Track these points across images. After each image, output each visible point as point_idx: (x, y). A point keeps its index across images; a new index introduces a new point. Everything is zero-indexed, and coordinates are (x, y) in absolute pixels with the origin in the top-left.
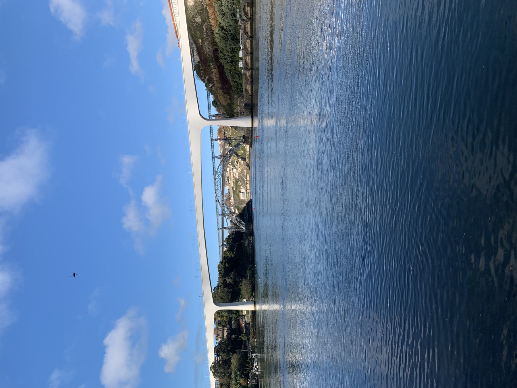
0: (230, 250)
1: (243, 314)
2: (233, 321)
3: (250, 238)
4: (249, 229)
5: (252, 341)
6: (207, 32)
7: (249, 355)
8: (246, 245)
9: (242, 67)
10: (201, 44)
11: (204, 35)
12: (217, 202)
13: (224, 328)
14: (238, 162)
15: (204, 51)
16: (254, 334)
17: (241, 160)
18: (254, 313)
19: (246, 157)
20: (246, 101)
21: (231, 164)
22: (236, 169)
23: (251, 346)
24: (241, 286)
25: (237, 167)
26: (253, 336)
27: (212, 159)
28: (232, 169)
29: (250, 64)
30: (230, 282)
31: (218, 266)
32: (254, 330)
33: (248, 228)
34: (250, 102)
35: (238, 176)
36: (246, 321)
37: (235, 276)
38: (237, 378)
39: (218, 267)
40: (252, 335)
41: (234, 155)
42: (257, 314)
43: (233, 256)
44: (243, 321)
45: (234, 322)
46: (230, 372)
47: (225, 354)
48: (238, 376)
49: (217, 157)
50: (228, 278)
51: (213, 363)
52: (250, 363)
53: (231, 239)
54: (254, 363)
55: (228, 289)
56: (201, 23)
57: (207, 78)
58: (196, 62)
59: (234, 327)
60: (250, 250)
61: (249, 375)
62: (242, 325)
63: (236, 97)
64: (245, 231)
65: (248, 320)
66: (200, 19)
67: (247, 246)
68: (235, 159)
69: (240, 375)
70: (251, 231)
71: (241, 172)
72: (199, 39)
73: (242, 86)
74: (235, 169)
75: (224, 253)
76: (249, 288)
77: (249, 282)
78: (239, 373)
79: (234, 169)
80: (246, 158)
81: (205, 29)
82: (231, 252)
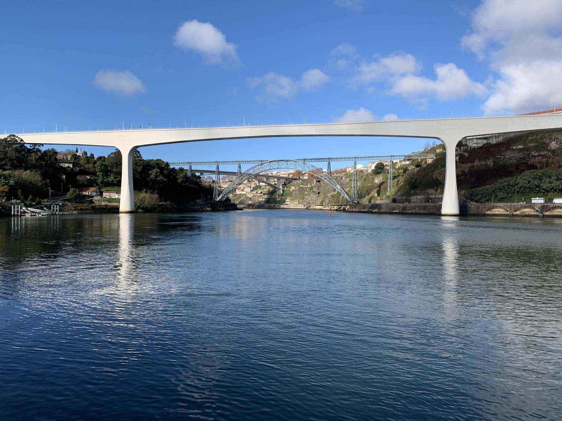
0: (186, 179)
1: (104, 194)
2: (89, 177)
3: (208, 207)
4: (218, 205)
5: (70, 206)
6: (539, 156)
7: (46, 200)
8: (198, 201)
9: (532, 202)
10: (515, 148)
11: (533, 152)
12: (260, 162)
13: (71, 163)
14: (262, 194)
15: (506, 151)
16: (81, 209)
17: (266, 197)
18: (115, 210)
19: (272, 205)
20: (472, 206)
21: (257, 186)
22: (250, 191)
23: (61, 204)
24: (146, 192)
25: (255, 192)
26: (78, 208)
27: (327, 157)
28: (250, 187)
29: (552, 214)
30: (151, 174)
31: (161, 160)
32: (88, 209)
33: (219, 205)
34: (472, 212)
35: (241, 194)
36: (92, 197)
37: (160, 182)
38: (2, 178)
39: (158, 160)
40: (79, 206)
41: (271, 189)
42: (116, 215)
43: (179, 181)
44: (93, 193)
45: (88, 180)
46: (6, 167)
47: (34, 161)
48: (7, 180)
49: (329, 164)
50: (158, 172)
51: (22, 140)
52: (34, 201)
53: (195, 180)
54: (35, 208)
55: (140, 171)
56: (549, 148)
57: (465, 154)
58: (466, 142)
59: (79, 178)
60: (192, 207)
61: (14, 199)
62: (86, 191)
63: (464, 192)
64: (215, 200)
65: (98, 201)
66: (555, 147)
67: (197, 202)
68: (265, 190)
69: (9, 183)
70: (217, 209)
71: (248, 197)
72: (522, 145)
73: (486, 201)
74: (251, 190)
75: (182, 170)
76: (146, 203)
77: (154, 204)
78: (12, 182)
79: (250, 189)
80: (270, 204)
81: (542, 153)
82: (184, 180)
